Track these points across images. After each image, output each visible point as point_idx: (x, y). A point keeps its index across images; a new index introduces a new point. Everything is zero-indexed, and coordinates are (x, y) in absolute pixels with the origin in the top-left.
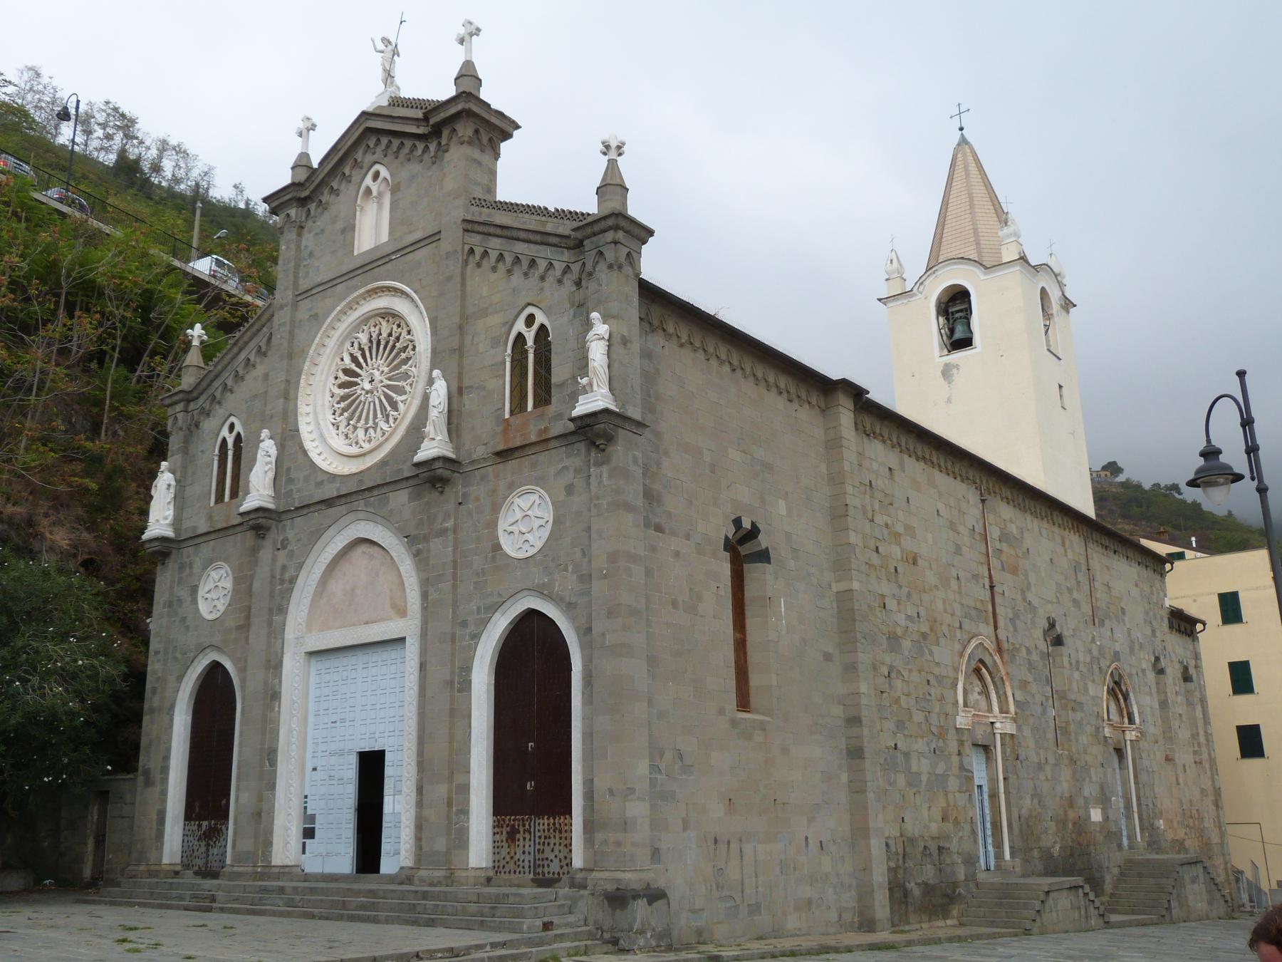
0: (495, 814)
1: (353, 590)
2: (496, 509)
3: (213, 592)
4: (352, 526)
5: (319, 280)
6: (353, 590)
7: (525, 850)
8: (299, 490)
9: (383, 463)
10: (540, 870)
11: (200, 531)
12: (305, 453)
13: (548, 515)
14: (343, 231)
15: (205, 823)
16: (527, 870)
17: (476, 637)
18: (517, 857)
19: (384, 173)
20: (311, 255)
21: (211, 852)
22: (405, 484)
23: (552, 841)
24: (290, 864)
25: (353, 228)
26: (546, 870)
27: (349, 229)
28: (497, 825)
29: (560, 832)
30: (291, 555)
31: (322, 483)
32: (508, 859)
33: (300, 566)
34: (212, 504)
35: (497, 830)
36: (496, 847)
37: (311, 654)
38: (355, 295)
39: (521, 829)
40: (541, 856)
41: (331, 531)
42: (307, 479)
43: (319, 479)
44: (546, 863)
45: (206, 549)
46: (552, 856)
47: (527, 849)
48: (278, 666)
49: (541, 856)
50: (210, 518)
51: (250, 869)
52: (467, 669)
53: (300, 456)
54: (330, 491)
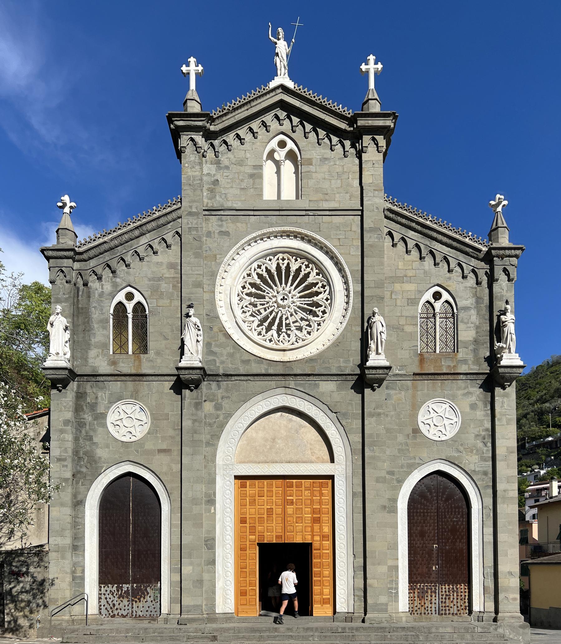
0: (409, 583)
1: (274, 440)
2: (415, 408)
3: (127, 421)
4: (278, 397)
5: (229, 205)
6: (274, 440)
7: (433, 601)
8: (222, 362)
9: (310, 360)
10: (443, 612)
11: (101, 371)
12: (228, 336)
13: (457, 420)
14: (252, 176)
15: (125, 587)
16: (434, 612)
17: (401, 482)
18: (426, 605)
19: (290, 145)
20: (216, 182)
21: (135, 605)
22: (335, 378)
23: (452, 597)
24: (230, 611)
25: (261, 176)
26: (447, 612)
27: (257, 176)
28: (412, 589)
29: (457, 592)
30: (218, 407)
31: (249, 361)
32: (419, 606)
33: (229, 416)
34: (111, 353)
35: (411, 591)
36: (412, 600)
37: (237, 477)
38: (271, 230)
39: (429, 591)
40: (444, 605)
41: (259, 397)
42: (231, 355)
43: (246, 357)
44: (447, 608)
45: (116, 386)
46: (452, 605)
47: (433, 601)
48: (213, 482)
49: (444, 605)
50: (114, 363)
51: (200, 616)
52: (395, 500)
53: (222, 339)
54: (255, 369)
